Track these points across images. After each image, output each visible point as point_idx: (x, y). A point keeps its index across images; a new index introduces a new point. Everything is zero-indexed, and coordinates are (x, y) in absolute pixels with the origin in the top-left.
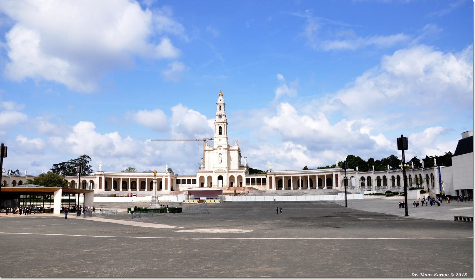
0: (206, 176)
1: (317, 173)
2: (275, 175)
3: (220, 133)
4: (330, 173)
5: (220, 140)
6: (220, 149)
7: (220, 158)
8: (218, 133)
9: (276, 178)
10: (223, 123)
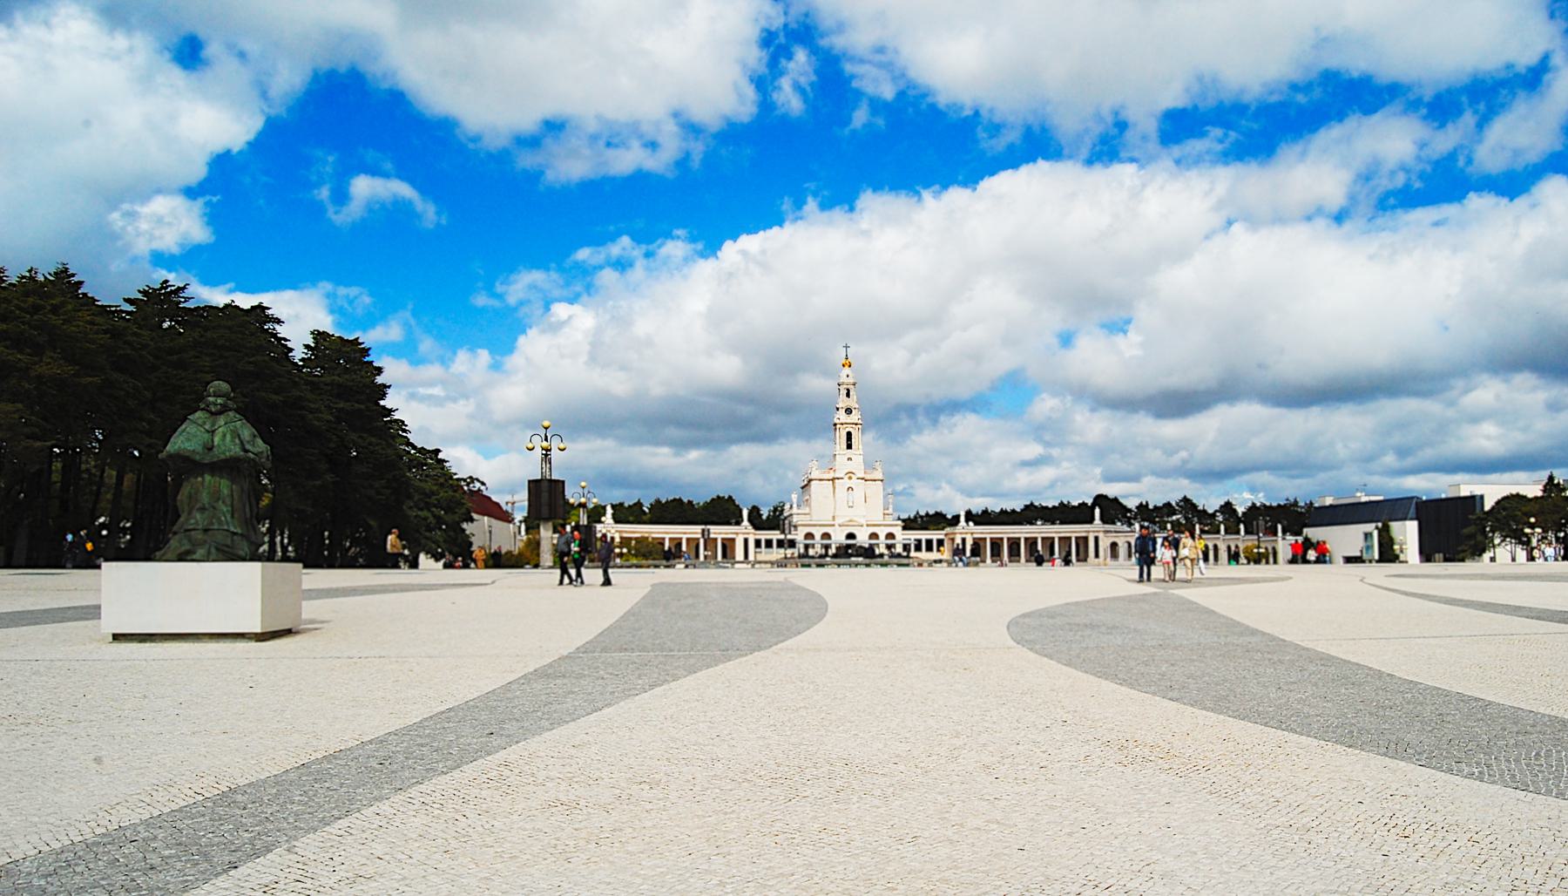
0: (818, 533)
1: (1056, 532)
2: (972, 534)
3: (849, 447)
4: (1084, 534)
5: (849, 459)
6: (850, 478)
7: (850, 497)
8: (845, 447)
9: (974, 539)
10: (856, 424)
